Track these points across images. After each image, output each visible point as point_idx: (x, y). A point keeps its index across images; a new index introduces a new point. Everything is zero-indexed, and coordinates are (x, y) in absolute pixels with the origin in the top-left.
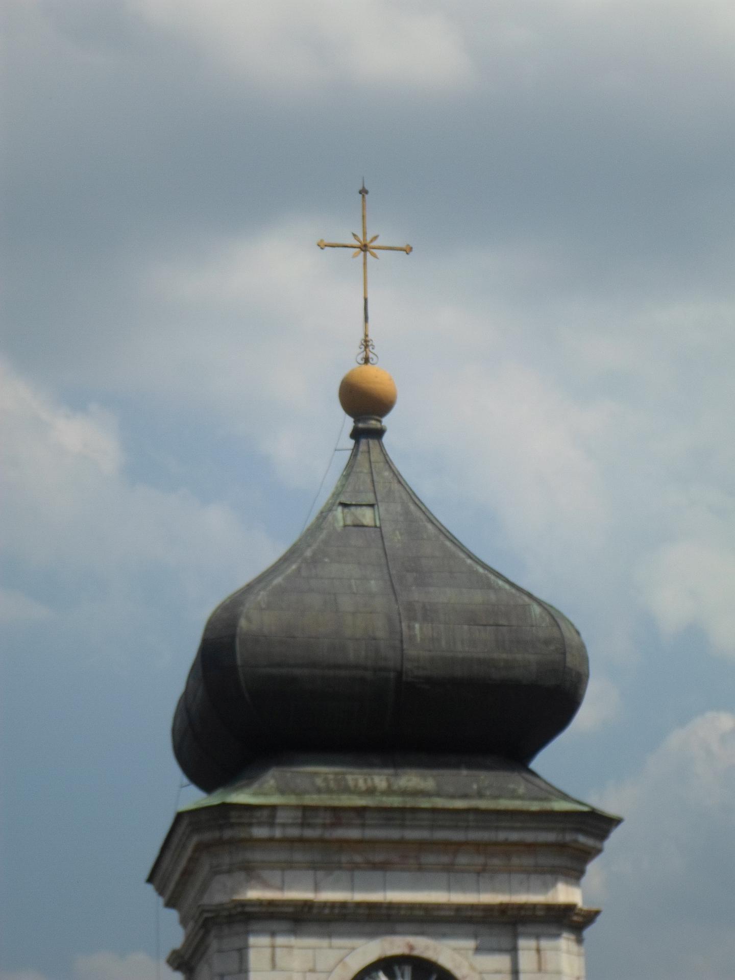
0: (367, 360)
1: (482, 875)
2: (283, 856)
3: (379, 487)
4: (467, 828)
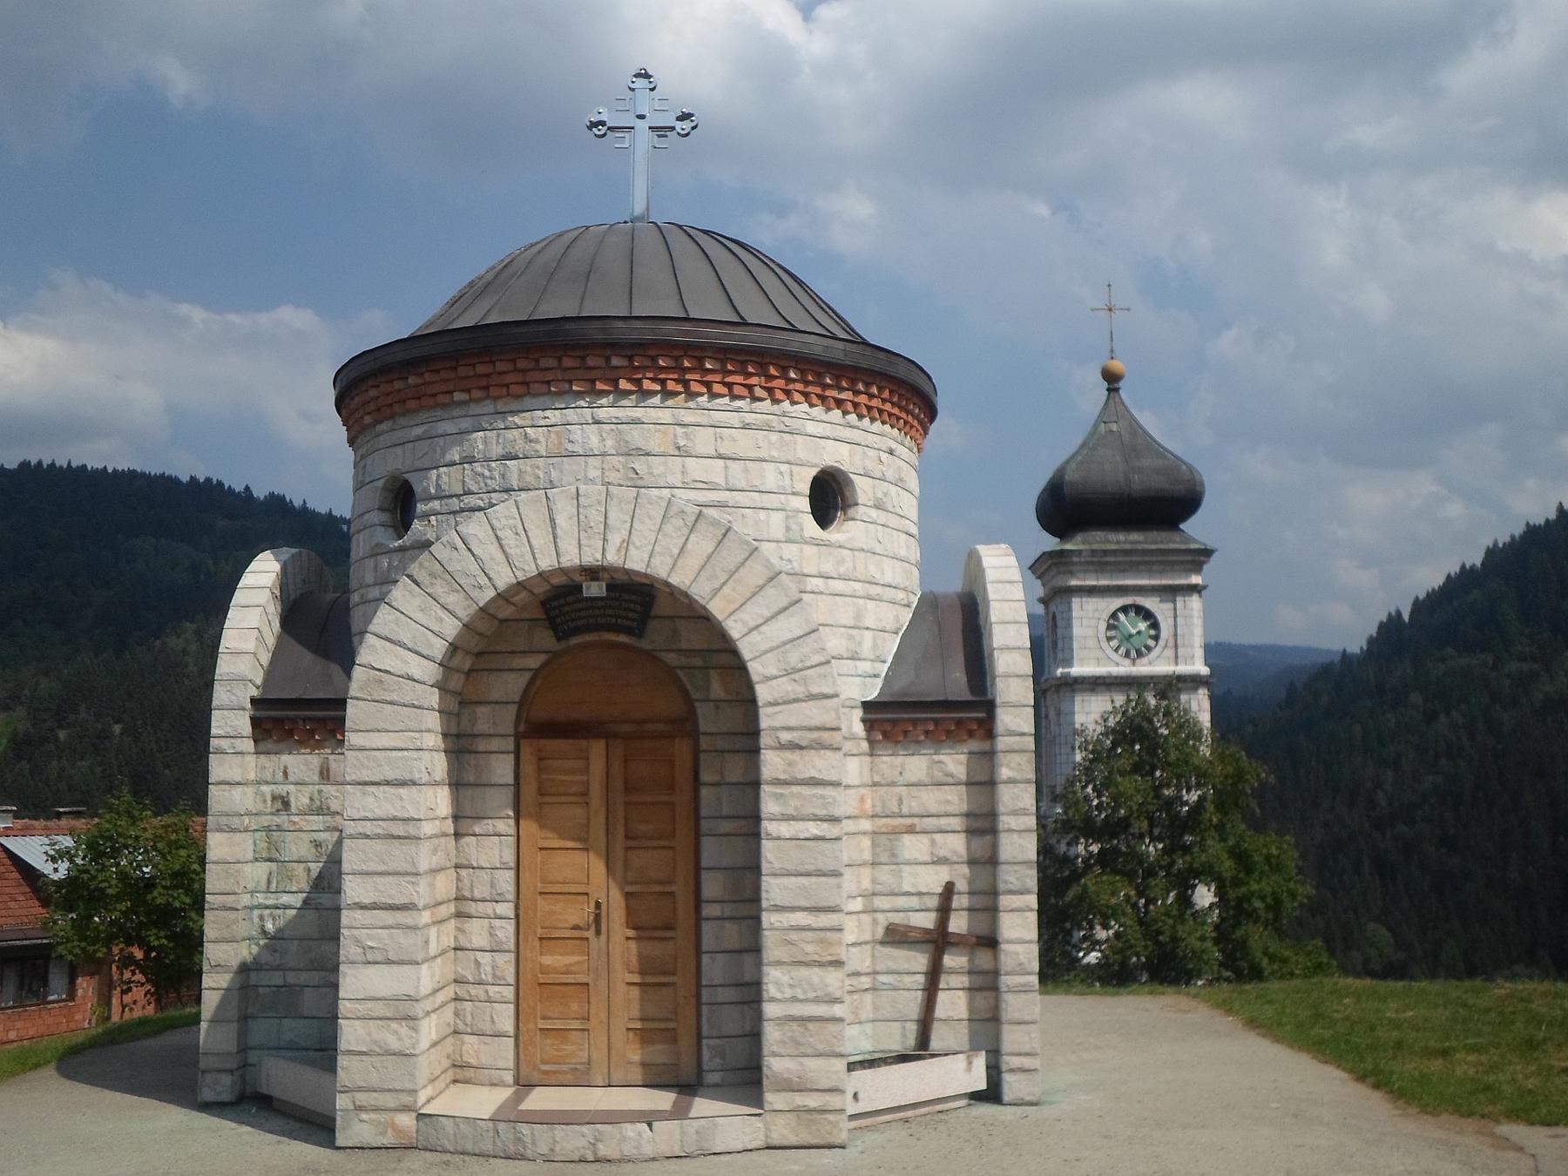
1: (1162, 573)
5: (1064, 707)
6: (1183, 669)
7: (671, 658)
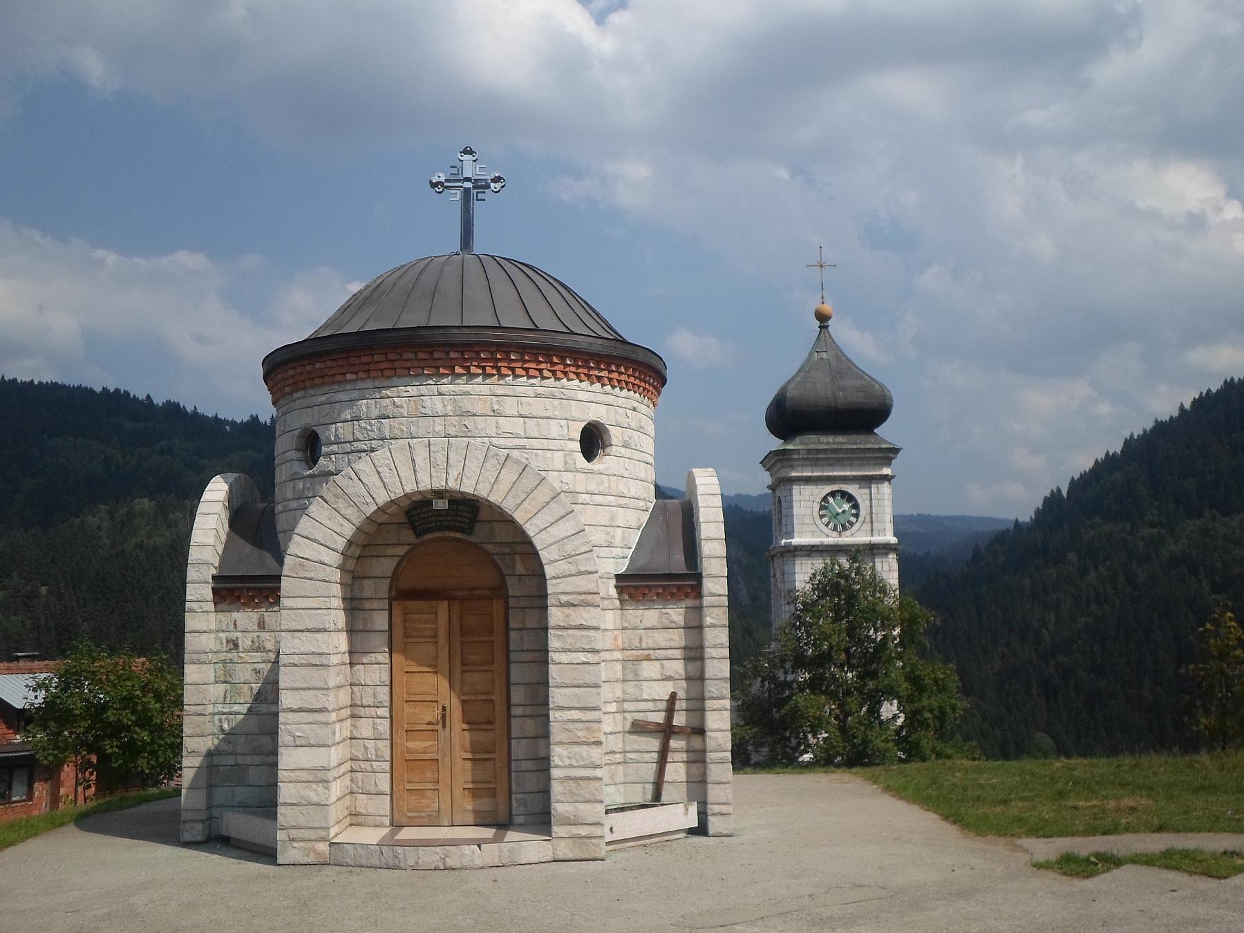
1: (861, 466)
5: (787, 568)
6: (876, 539)
7: (490, 548)
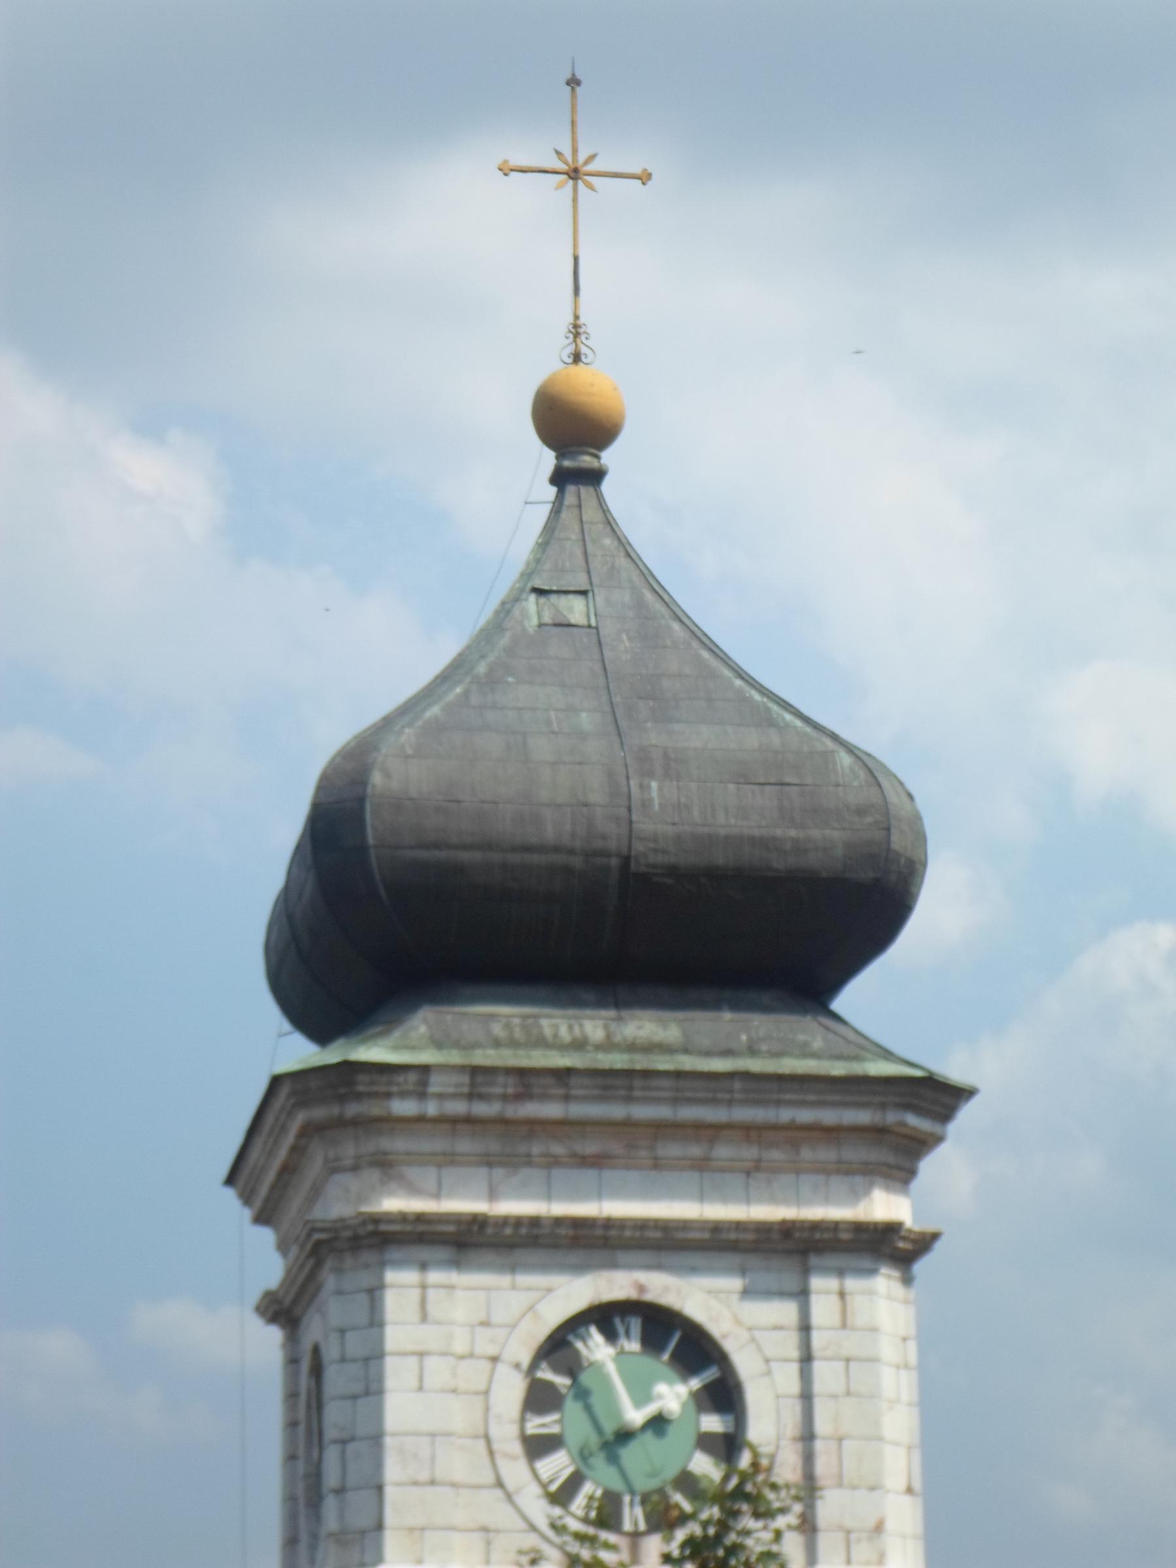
0: (577, 358)
2: (439, 1144)
3: (595, 563)
4: (730, 1103)
